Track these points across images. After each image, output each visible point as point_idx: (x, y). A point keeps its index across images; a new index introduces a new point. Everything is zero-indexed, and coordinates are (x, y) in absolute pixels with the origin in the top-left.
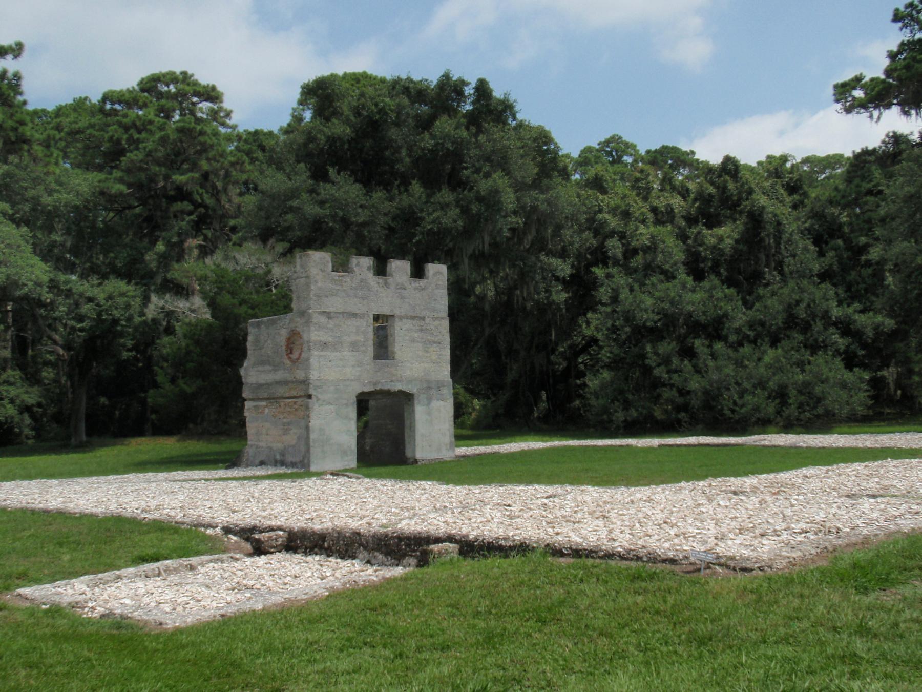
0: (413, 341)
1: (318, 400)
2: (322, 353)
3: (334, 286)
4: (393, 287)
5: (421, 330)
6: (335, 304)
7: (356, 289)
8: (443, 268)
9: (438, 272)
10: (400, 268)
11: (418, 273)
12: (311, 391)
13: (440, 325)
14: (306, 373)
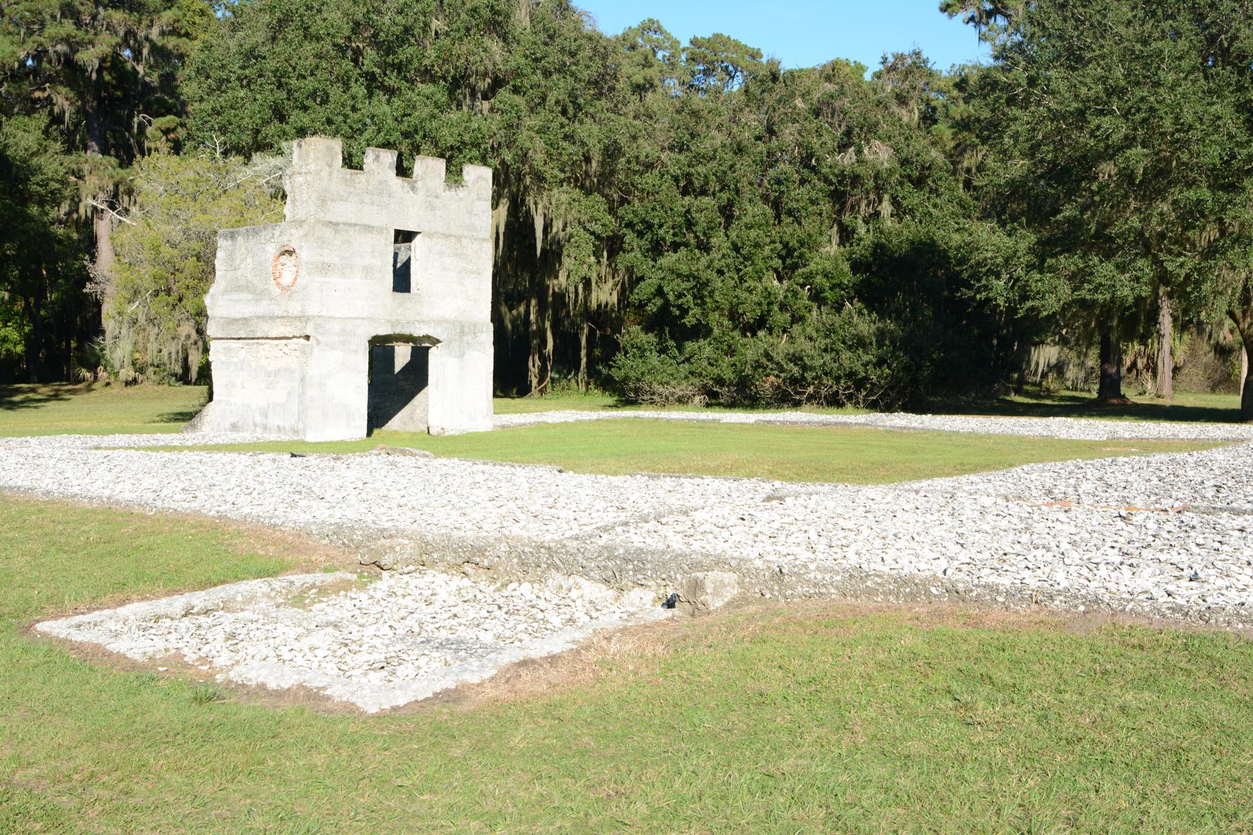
1: (319, 343)
4: (421, 193)
10: (429, 168)
11: (454, 174)
14: (303, 306)
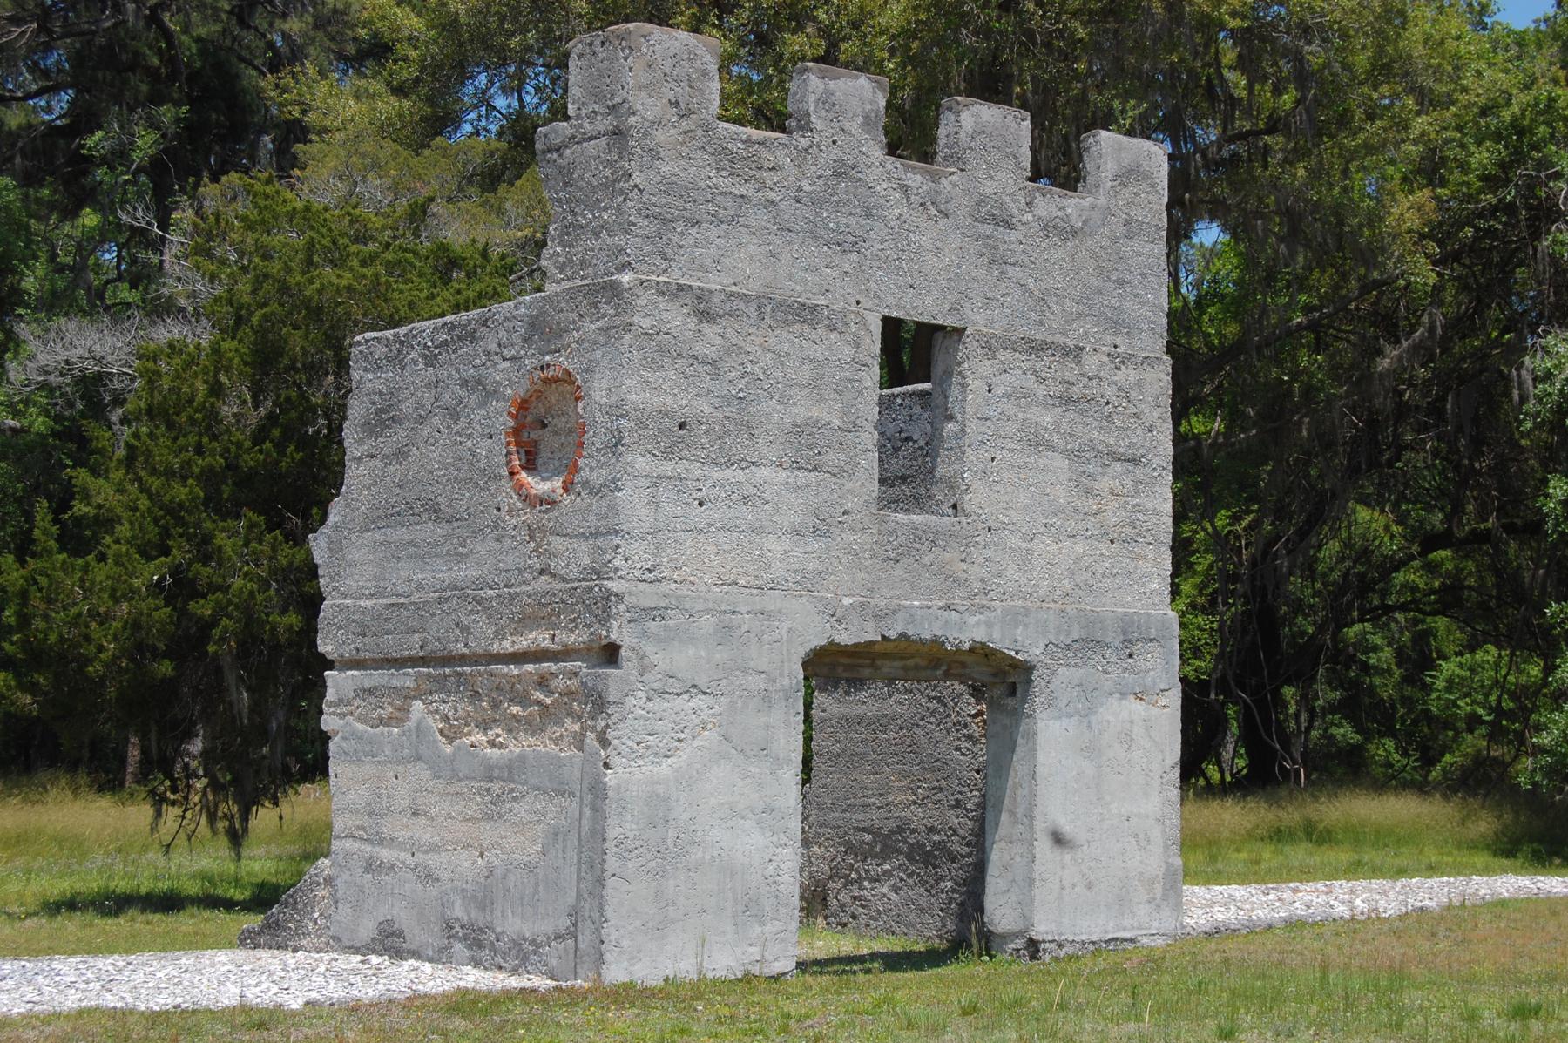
0: (1036, 443)
2: (668, 468)
3: (724, 182)
5: (1066, 401)
6: (735, 260)
7: (817, 202)
8: (1155, 155)
9: (1130, 165)
11: (1057, 165)
12: (618, 632)
13: (1140, 384)
